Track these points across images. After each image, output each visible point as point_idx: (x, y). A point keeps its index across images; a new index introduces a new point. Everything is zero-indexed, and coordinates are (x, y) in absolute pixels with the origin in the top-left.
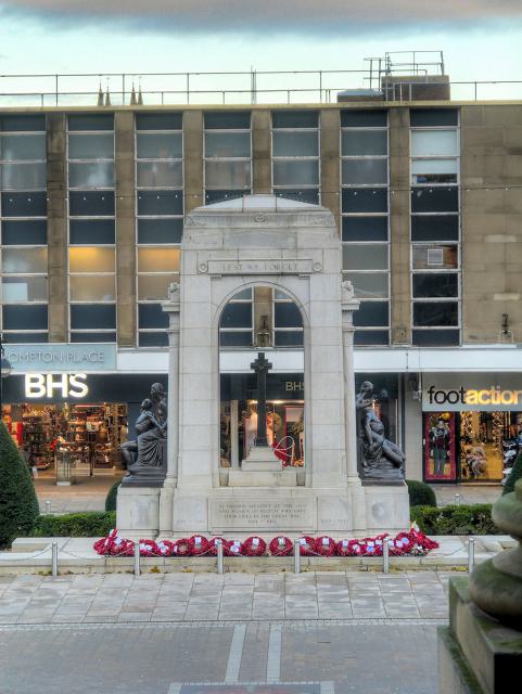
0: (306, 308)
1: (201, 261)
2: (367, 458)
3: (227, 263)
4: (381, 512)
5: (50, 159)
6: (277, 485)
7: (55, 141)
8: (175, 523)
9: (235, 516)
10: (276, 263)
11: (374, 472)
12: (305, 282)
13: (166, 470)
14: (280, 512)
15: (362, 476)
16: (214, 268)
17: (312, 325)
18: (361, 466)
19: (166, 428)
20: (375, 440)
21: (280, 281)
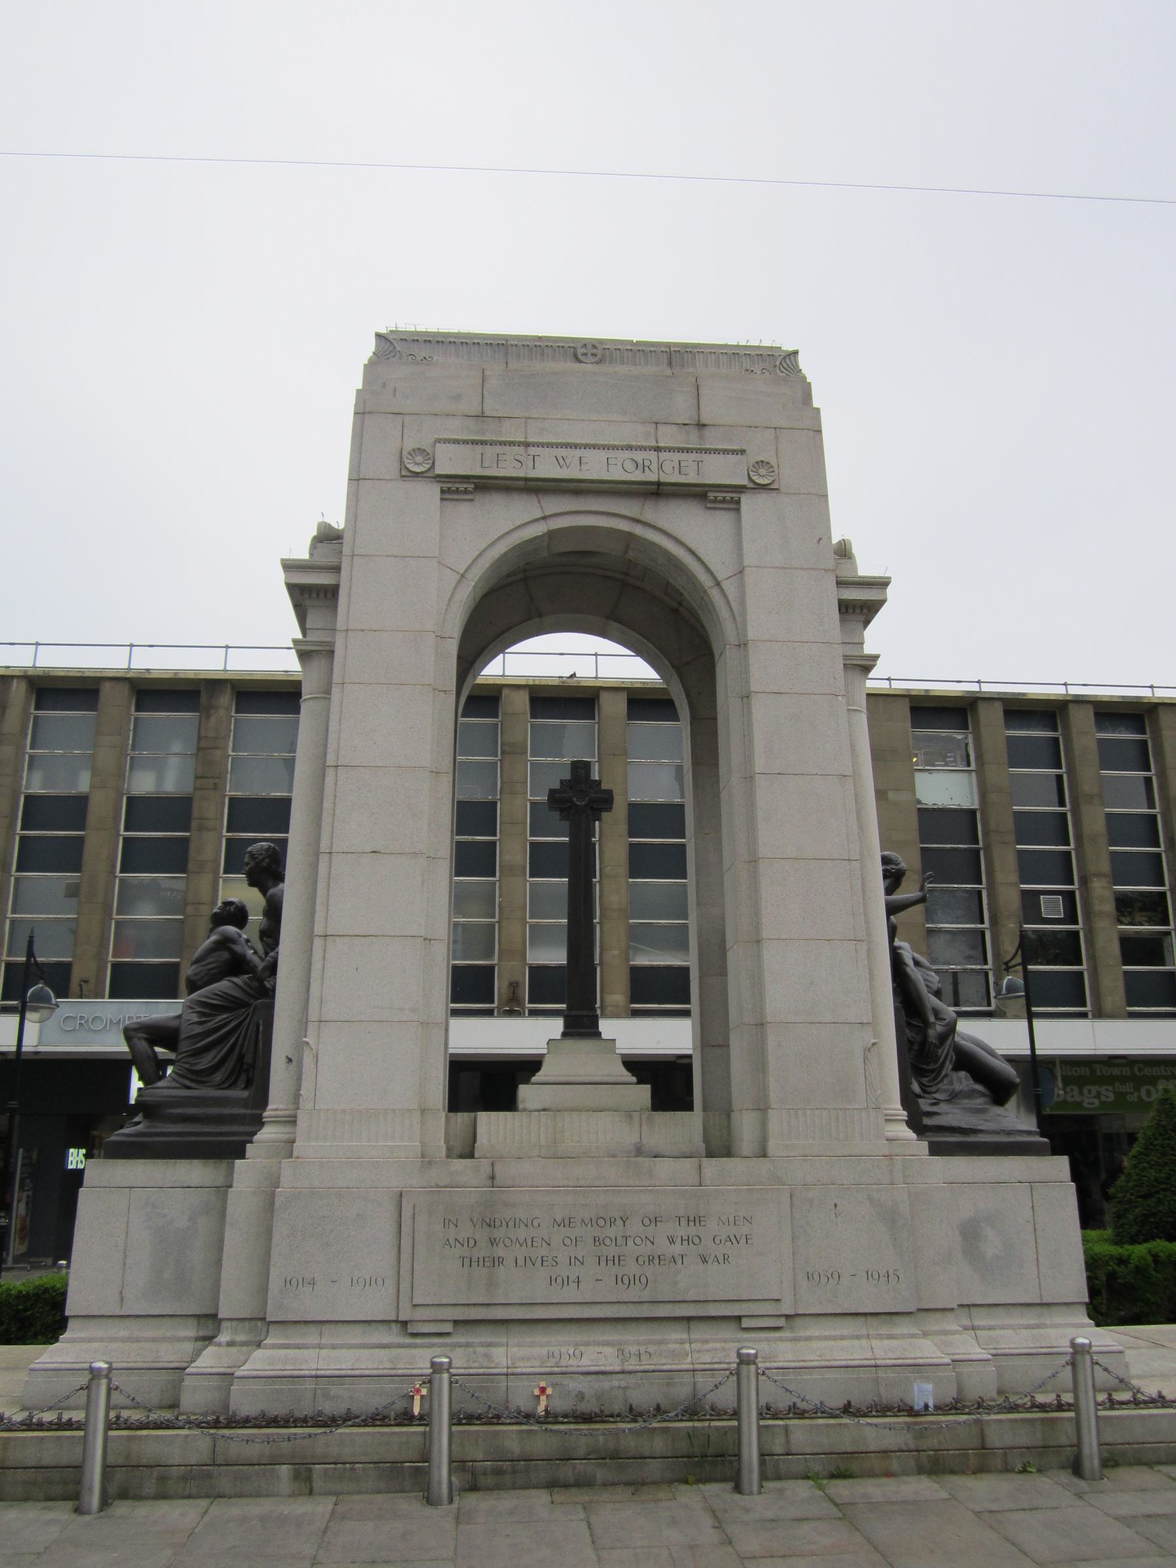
0: (730, 587)
1: (410, 444)
2: (919, 1072)
3: (490, 451)
4: (992, 1246)
5: (203, 744)
6: (639, 1151)
7: (213, 719)
8: (275, 1284)
9: (497, 1262)
10: (639, 456)
11: (951, 1115)
12: (722, 520)
13: (262, 1100)
14: (663, 1246)
15: (916, 1122)
16: (451, 462)
17: (751, 635)
18: (908, 1099)
19: (273, 968)
20: (936, 1013)
21: (652, 512)
